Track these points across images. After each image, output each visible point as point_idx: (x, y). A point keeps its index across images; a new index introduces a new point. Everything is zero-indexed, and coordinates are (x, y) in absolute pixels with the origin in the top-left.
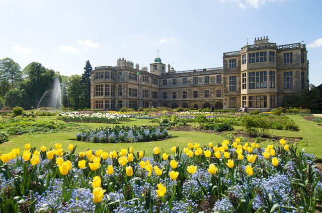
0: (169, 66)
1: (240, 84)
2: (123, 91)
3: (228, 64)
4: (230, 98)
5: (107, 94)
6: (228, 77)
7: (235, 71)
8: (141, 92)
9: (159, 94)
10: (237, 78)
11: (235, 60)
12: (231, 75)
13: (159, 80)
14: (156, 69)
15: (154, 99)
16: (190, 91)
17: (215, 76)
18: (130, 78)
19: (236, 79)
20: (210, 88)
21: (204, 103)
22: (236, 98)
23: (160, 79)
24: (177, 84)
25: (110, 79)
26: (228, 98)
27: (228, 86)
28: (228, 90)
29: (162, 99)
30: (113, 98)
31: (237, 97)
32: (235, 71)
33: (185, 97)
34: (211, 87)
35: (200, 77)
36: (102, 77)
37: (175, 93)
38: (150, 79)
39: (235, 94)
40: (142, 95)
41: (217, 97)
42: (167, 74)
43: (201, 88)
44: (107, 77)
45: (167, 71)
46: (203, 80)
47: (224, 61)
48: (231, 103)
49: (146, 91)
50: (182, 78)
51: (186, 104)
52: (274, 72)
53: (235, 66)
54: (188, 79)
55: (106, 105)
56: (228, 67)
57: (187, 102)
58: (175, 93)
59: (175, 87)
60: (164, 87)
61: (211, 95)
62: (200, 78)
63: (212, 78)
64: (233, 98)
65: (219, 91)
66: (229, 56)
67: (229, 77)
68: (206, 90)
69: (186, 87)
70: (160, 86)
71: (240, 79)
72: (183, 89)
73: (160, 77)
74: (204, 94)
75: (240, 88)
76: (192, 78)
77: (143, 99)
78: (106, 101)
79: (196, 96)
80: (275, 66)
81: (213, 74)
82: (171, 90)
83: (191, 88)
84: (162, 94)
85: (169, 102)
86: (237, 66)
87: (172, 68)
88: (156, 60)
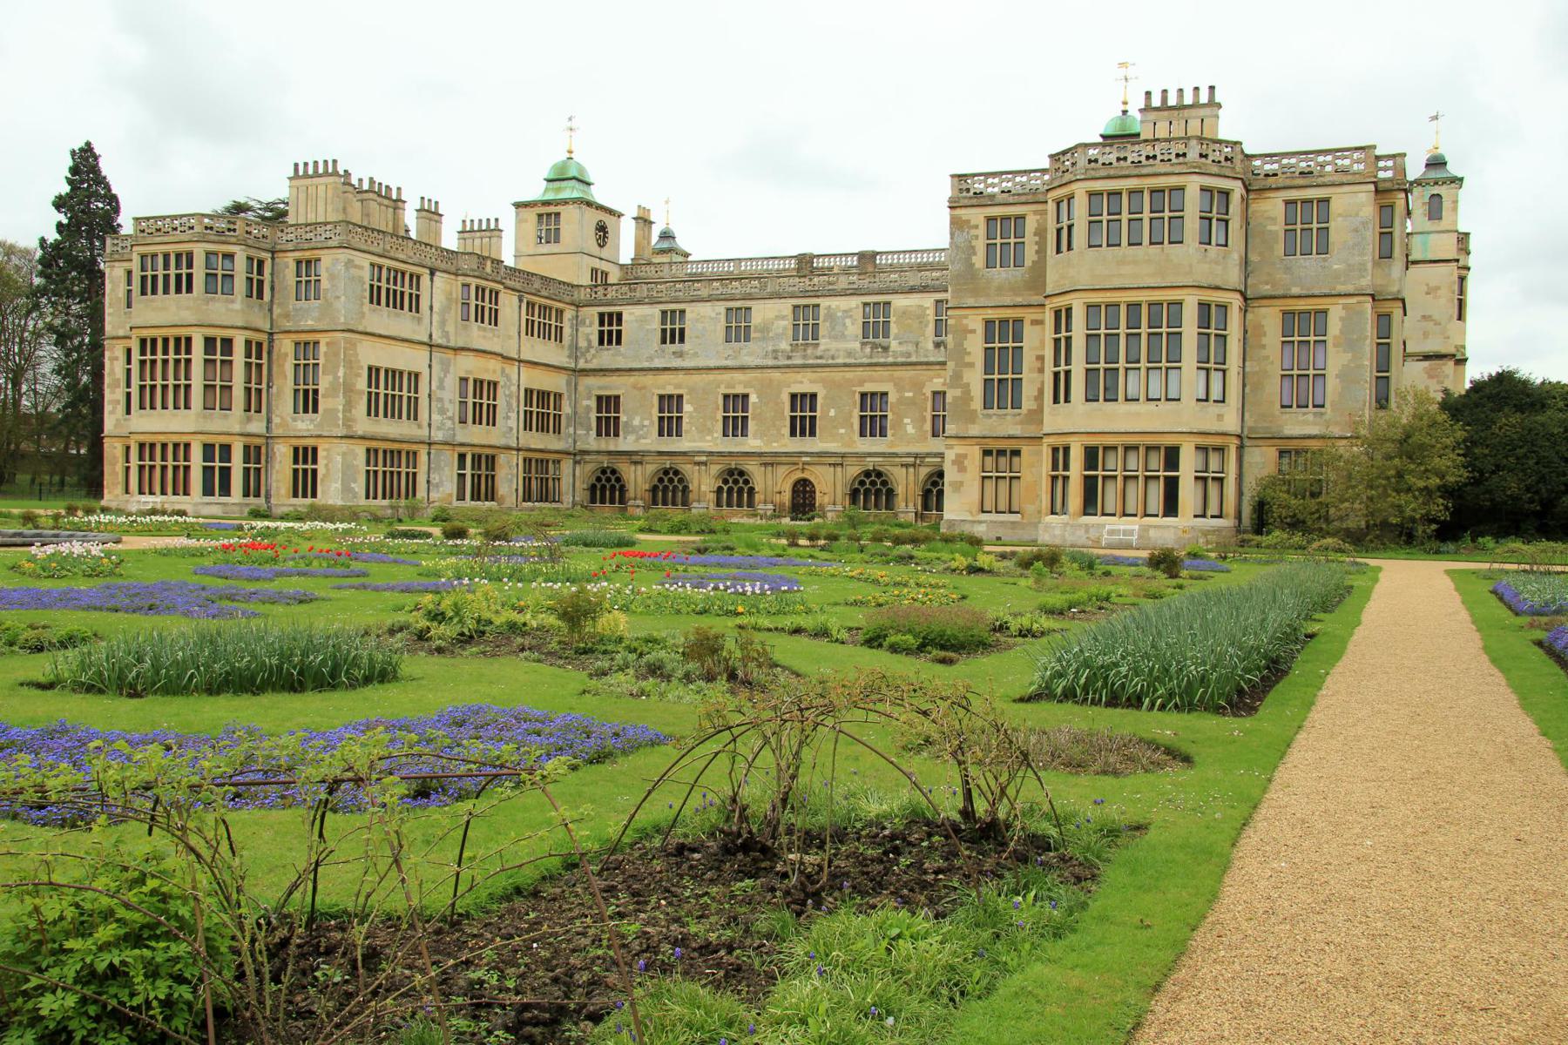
0: (644, 221)
1: (1041, 370)
2: (323, 387)
3: (981, 245)
4: (987, 453)
5: (218, 395)
6: (976, 322)
7: (1014, 290)
8: (450, 394)
9: (566, 409)
10: (1028, 330)
12: (992, 314)
13: (569, 314)
14: (553, 236)
15: (536, 440)
18: (375, 296)
19: (1018, 337)
20: (900, 389)
21: (854, 471)
23: (578, 306)
24: (687, 346)
25: (237, 306)
26: (976, 452)
28: (977, 403)
29: (591, 441)
30: (257, 426)
31: (1025, 450)
32: (1014, 290)
33: (736, 425)
34: (900, 373)
36: (184, 284)
37: (671, 402)
38: (509, 306)
39: (1016, 430)
40: (453, 410)
42: (631, 275)
43: (837, 375)
44: (218, 282)
45: (626, 255)
46: (854, 328)
47: (957, 225)
48: (990, 485)
49: (479, 383)
50: (721, 308)
51: (741, 473)
52: (1223, 308)
55: (208, 471)
56: (979, 260)
58: (671, 402)
60: (608, 357)
61: (899, 424)
62: (830, 316)
63: (905, 313)
66: (980, 200)
67: (980, 328)
68: (869, 387)
69: (742, 368)
70: (575, 351)
71: (1042, 343)
72: (727, 376)
73: (583, 295)
74: (857, 413)
75: (1041, 391)
76: (785, 307)
77: (460, 438)
78: (208, 450)
79: (803, 425)
80: (1234, 277)
81: (912, 290)
82: (648, 379)
83: (776, 375)
84: (593, 403)
85: (635, 458)
86: (1028, 263)
87: (666, 236)
88: (558, 178)
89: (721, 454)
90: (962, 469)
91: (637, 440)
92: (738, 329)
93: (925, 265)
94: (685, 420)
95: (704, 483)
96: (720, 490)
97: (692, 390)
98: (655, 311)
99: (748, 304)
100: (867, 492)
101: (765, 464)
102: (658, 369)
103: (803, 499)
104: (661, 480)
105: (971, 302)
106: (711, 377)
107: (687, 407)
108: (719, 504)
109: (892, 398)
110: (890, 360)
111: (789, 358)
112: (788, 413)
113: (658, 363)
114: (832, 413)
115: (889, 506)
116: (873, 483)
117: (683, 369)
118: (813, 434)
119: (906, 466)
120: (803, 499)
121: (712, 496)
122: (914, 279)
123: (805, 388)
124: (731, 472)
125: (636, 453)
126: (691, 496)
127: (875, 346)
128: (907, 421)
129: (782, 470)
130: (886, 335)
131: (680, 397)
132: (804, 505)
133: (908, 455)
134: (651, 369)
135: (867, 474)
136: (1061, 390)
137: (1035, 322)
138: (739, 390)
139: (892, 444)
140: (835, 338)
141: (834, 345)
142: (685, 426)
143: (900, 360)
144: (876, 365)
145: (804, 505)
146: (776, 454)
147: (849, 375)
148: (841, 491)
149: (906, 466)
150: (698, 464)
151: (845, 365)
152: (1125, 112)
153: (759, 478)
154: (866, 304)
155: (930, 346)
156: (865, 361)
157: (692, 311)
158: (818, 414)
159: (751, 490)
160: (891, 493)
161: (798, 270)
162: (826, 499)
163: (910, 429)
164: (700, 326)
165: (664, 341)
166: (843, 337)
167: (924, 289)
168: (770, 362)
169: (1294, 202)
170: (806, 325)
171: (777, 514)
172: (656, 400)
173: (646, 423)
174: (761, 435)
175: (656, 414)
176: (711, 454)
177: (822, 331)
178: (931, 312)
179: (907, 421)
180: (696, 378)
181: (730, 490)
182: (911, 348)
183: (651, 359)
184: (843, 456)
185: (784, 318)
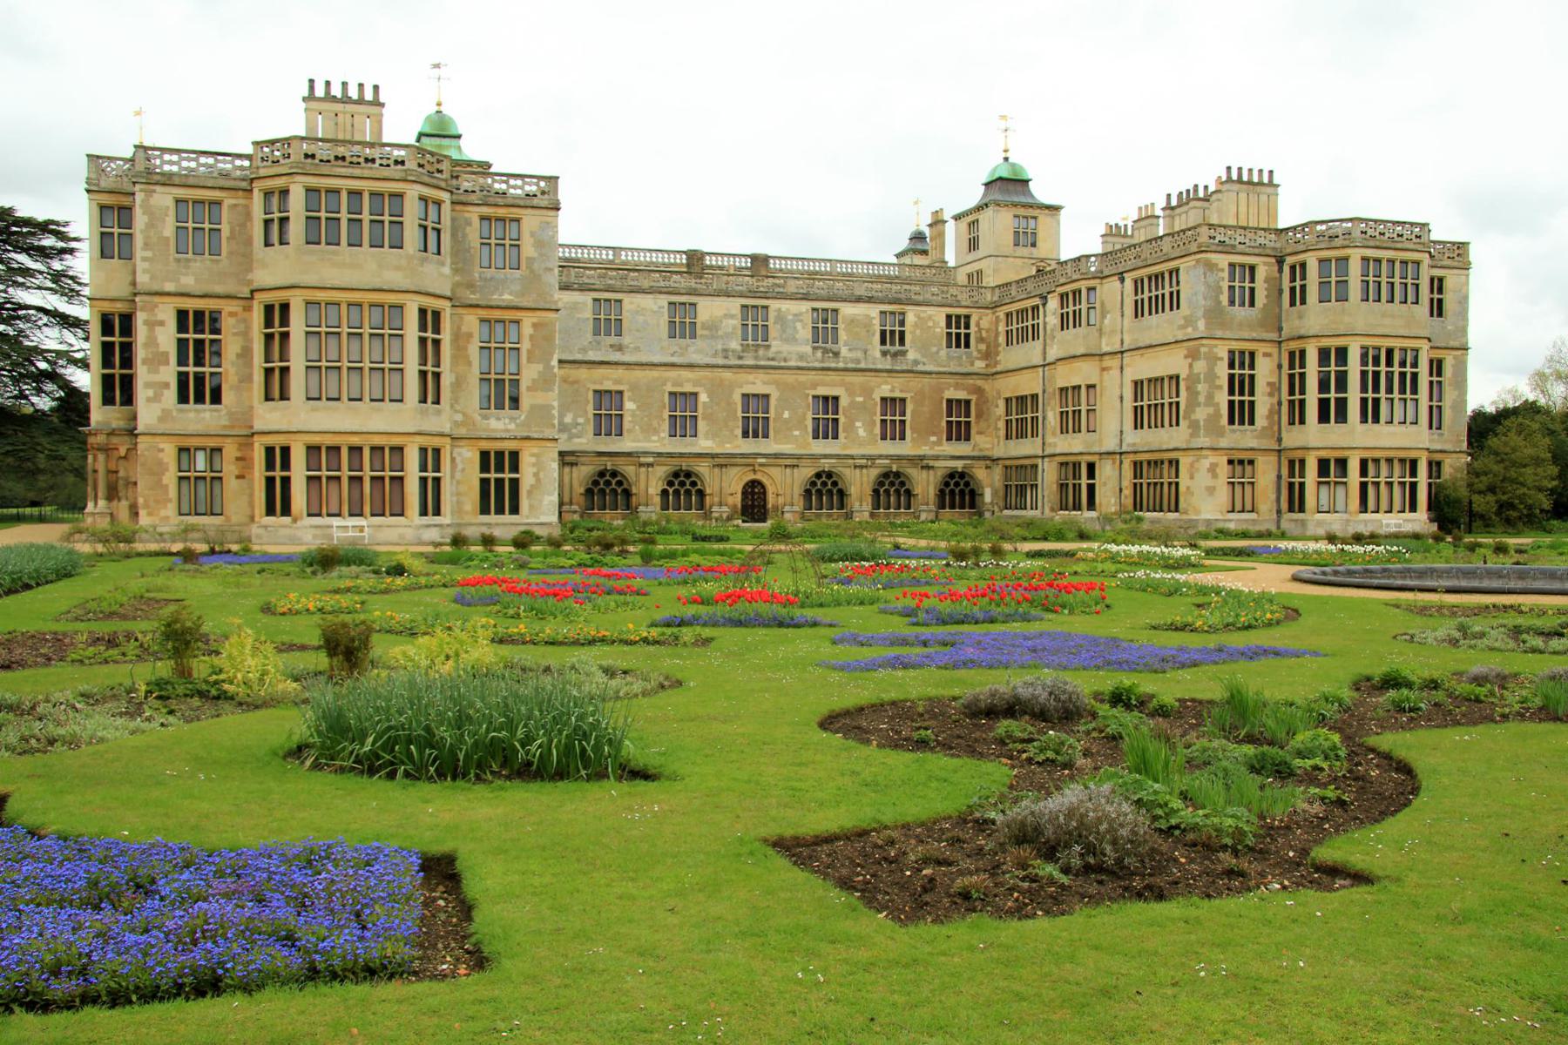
3: (1225, 285)
4: (1230, 462)
10: (1260, 361)
11: (1252, 269)
12: (1236, 346)
16: (716, 389)
17: (873, 311)
19: (1252, 367)
20: (851, 393)
21: (807, 472)
22: (1251, 462)
24: (626, 340)
27: (1223, 398)
35: (785, 306)
39: (1253, 444)
41: (884, 438)
43: (790, 378)
46: (804, 333)
50: (663, 301)
51: (688, 474)
53: (1252, 304)
54: (709, 309)
56: (1224, 299)
57: (703, 468)
59: (616, 356)
61: (851, 427)
62: (781, 318)
63: (852, 321)
64: (1241, 462)
65: (892, 404)
67: (1225, 356)
69: (691, 366)
74: (810, 416)
79: (755, 428)
81: (859, 300)
82: (582, 373)
83: (727, 375)
89: (670, 455)
90: (1215, 476)
91: (570, 438)
92: (682, 325)
93: (817, 273)
94: (627, 419)
95: (649, 485)
96: (664, 493)
97: (634, 387)
98: (587, 298)
99: (693, 299)
100: (819, 492)
101: (721, 466)
102: (594, 363)
103: (754, 503)
104: (596, 483)
105: (1219, 334)
106: (655, 373)
107: (629, 405)
108: (665, 507)
109: (843, 402)
110: (841, 365)
111: (740, 358)
112: (740, 414)
113: (592, 356)
114: (786, 415)
115: (842, 506)
116: (824, 484)
117: (623, 364)
118: (766, 436)
119: (862, 467)
120: (754, 503)
121: (657, 500)
122: (860, 291)
123: (759, 389)
124: (676, 475)
125: (572, 453)
126: (634, 499)
127: (826, 351)
128: (858, 424)
129: (735, 470)
130: (836, 341)
131: (621, 393)
132: (753, 506)
133: (863, 457)
134: (586, 362)
135: (818, 475)
136: (1297, 414)
137: (1266, 355)
138: (688, 388)
139: (845, 447)
140: (786, 341)
141: (786, 348)
142: (626, 425)
143: (851, 365)
144: (829, 369)
145: (753, 506)
146: (733, 456)
147: (802, 378)
148: (798, 491)
149: (862, 467)
150: (641, 465)
151: (799, 368)
152: (1006, 159)
153: (711, 479)
154: (814, 309)
155: (878, 355)
156: (817, 365)
157: (630, 302)
158: (772, 415)
159: (701, 494)
160: (842, 494)
161: (688, 265)
162: (781, 500)
163: (861, 432)
164: (641, 319)
165: (597, 332)
166: (793, 340)
167: (870, 300)
168: (721, 361)
169: (317, 190)
170: (756, 325)
171: (729, 519)
172: (591, 394)
173: (581, 420)
174: (712, 435)
175: (591, 410)
176: (660, 454)
177: (774, 331)
178: (876, 322)
179: (858, 424)
180: (638, 374)
181: (677, 492)
182: (859, 354)
183: (584, 350)
184: (799, 457)
185: (733, 317)
